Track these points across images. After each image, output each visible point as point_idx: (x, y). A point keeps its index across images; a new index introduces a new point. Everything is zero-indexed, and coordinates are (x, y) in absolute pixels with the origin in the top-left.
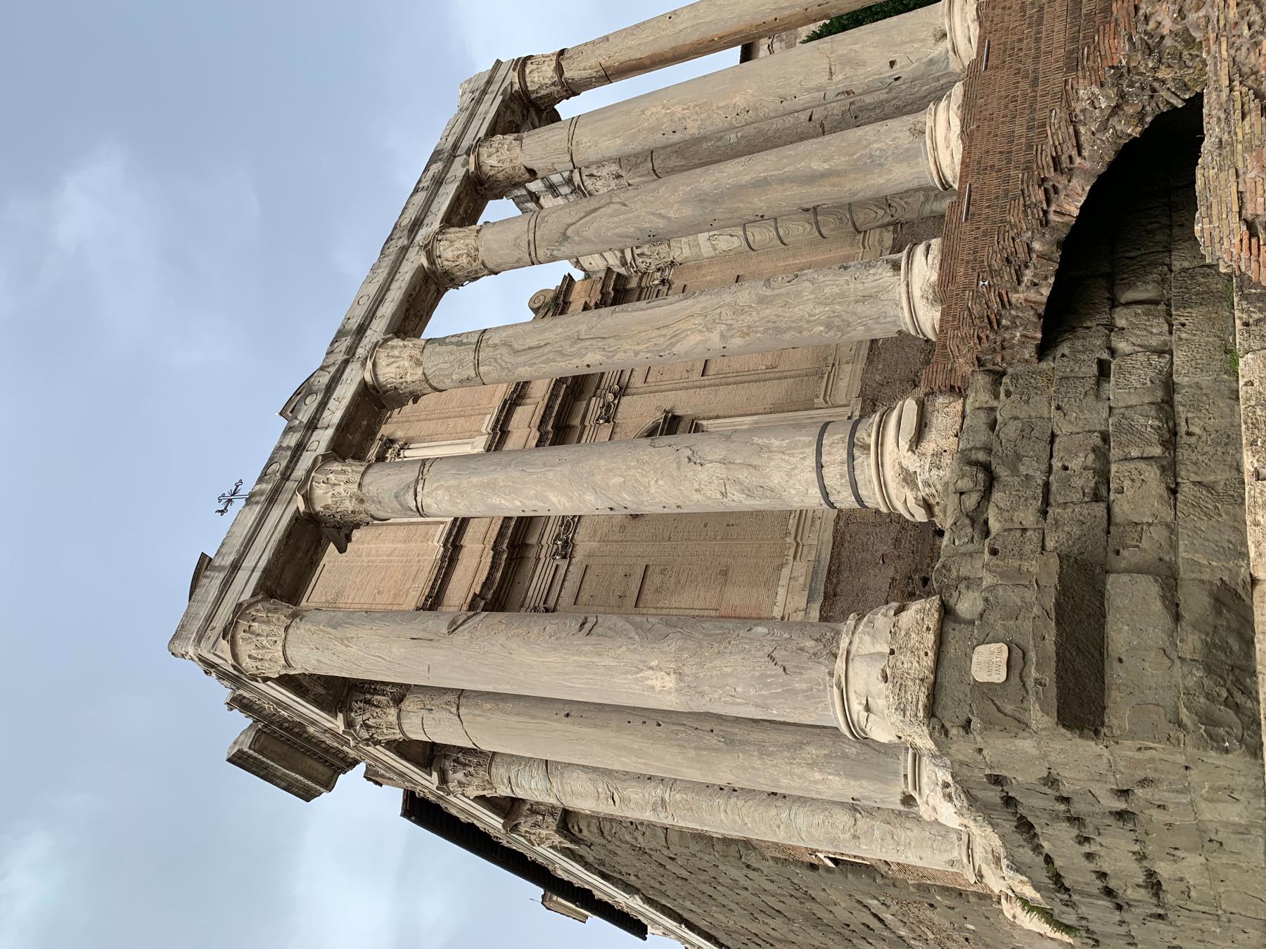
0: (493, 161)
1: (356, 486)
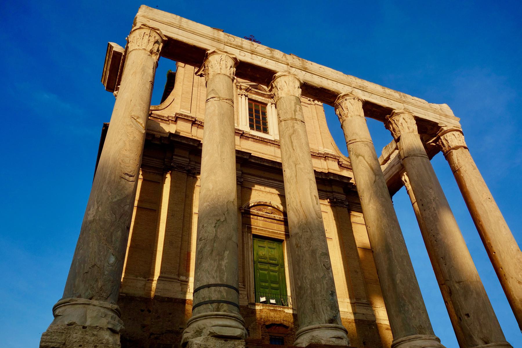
0: (401, 120)
1: (219, 72)
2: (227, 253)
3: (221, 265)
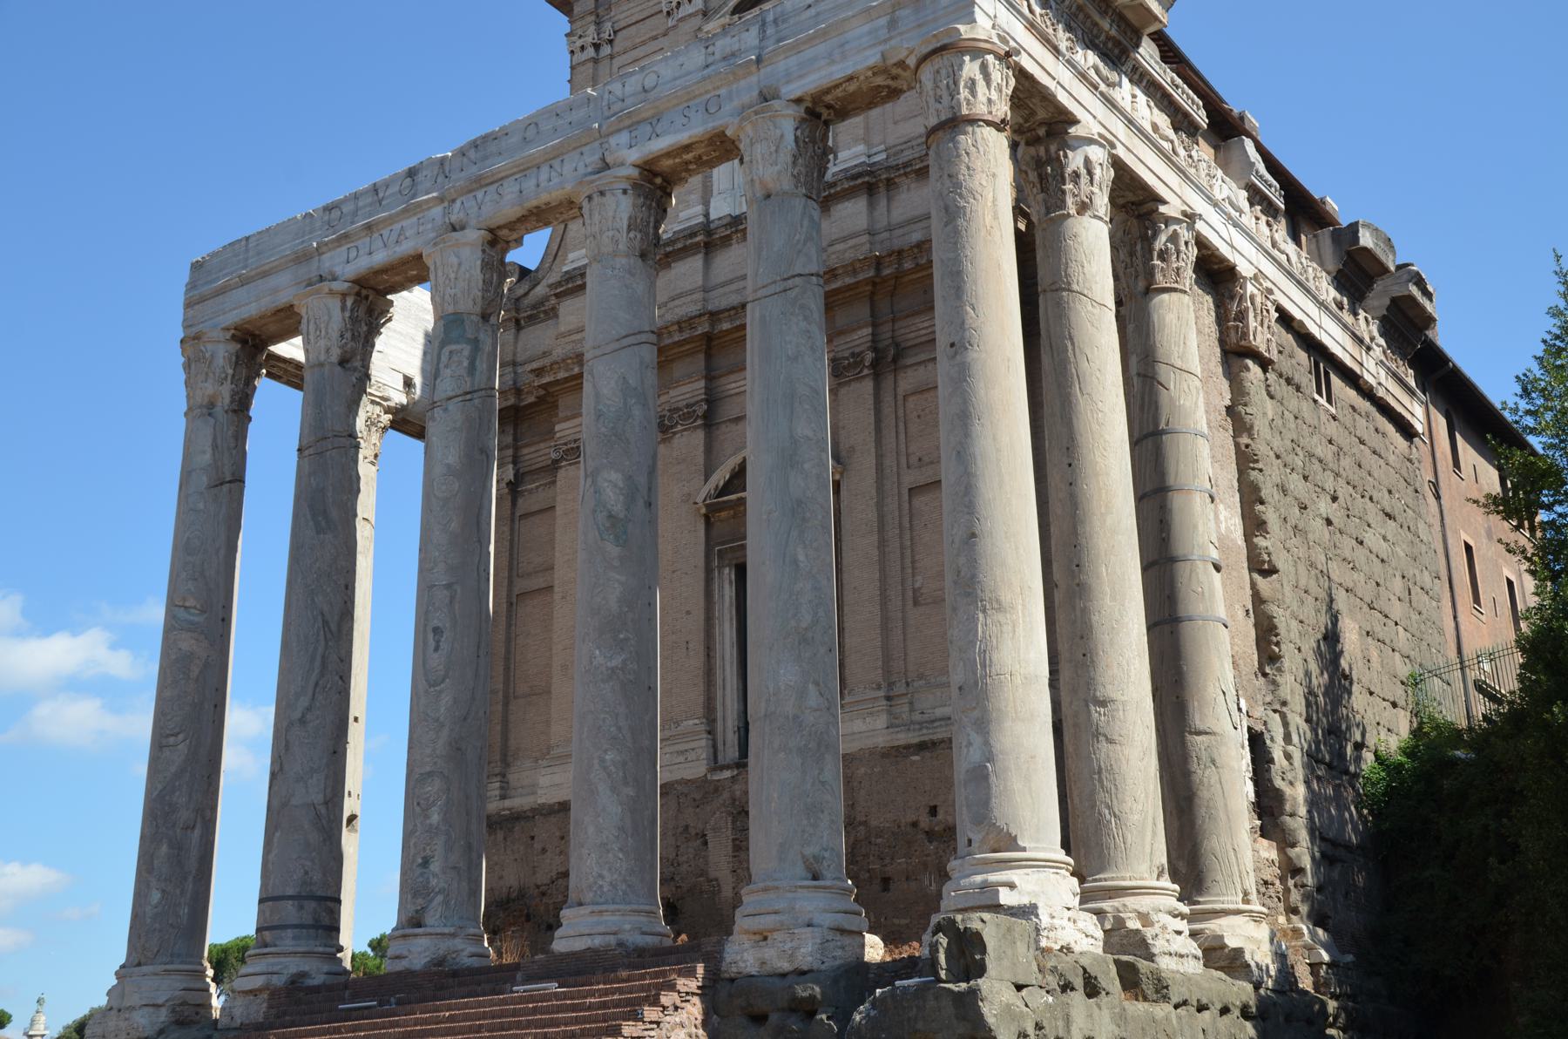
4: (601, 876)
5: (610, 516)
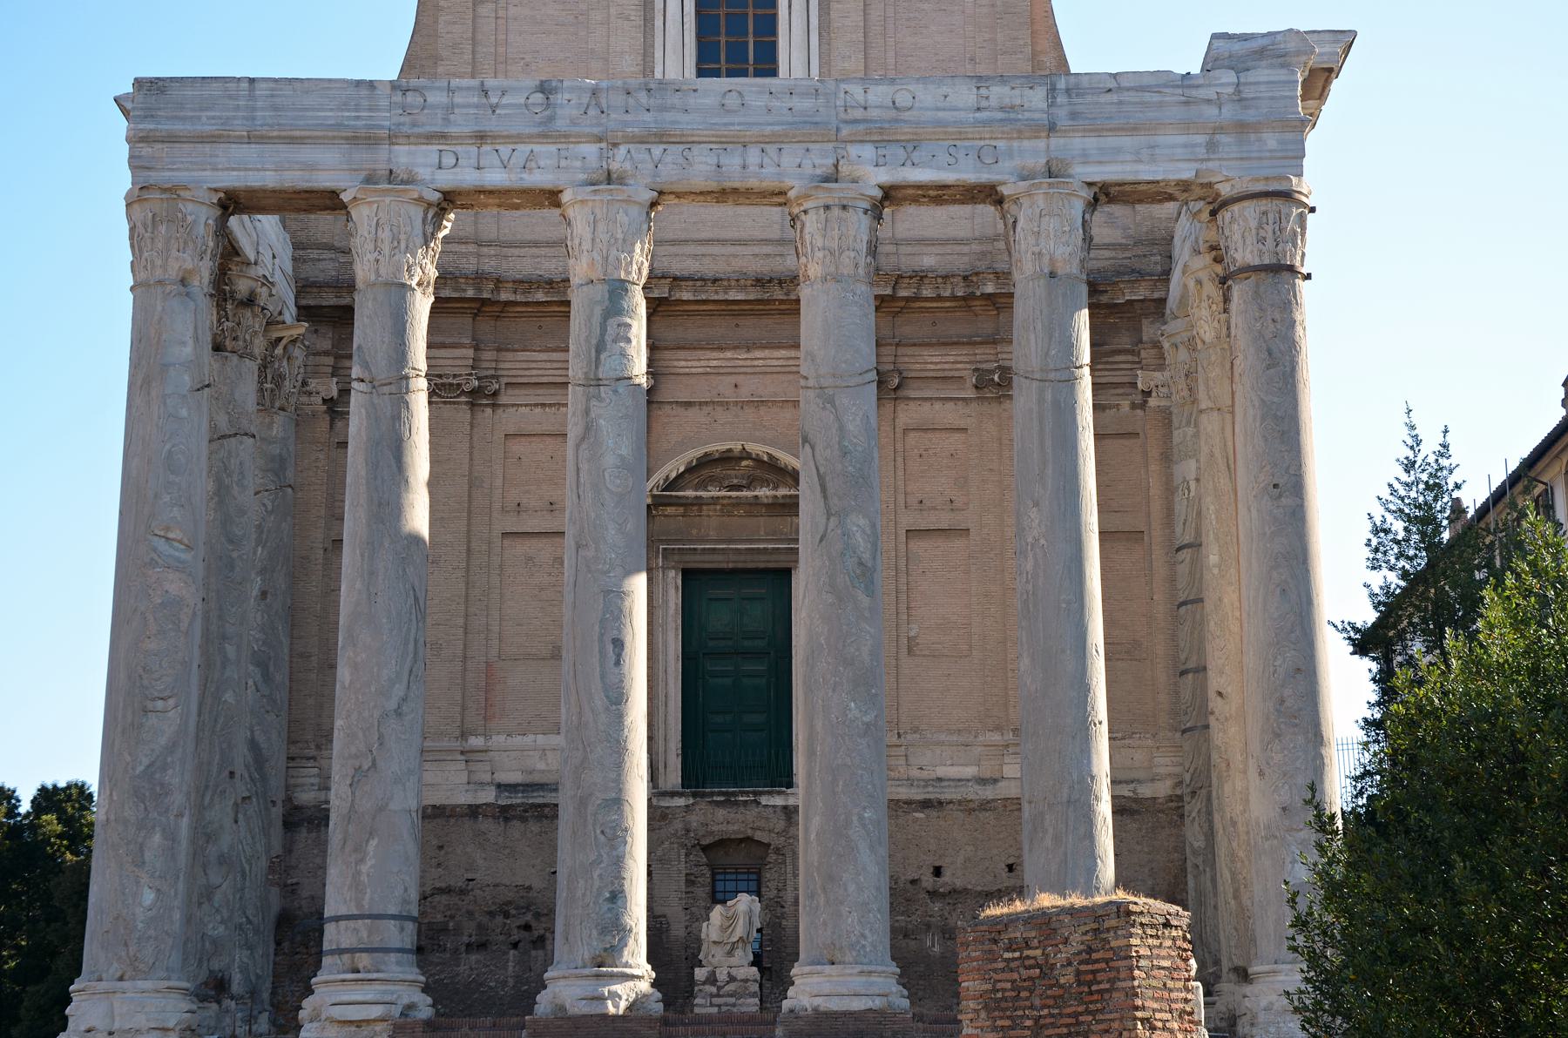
2: (374, 843)
3: (359, 873)
4: (863, 936)
5: (861, 564)
